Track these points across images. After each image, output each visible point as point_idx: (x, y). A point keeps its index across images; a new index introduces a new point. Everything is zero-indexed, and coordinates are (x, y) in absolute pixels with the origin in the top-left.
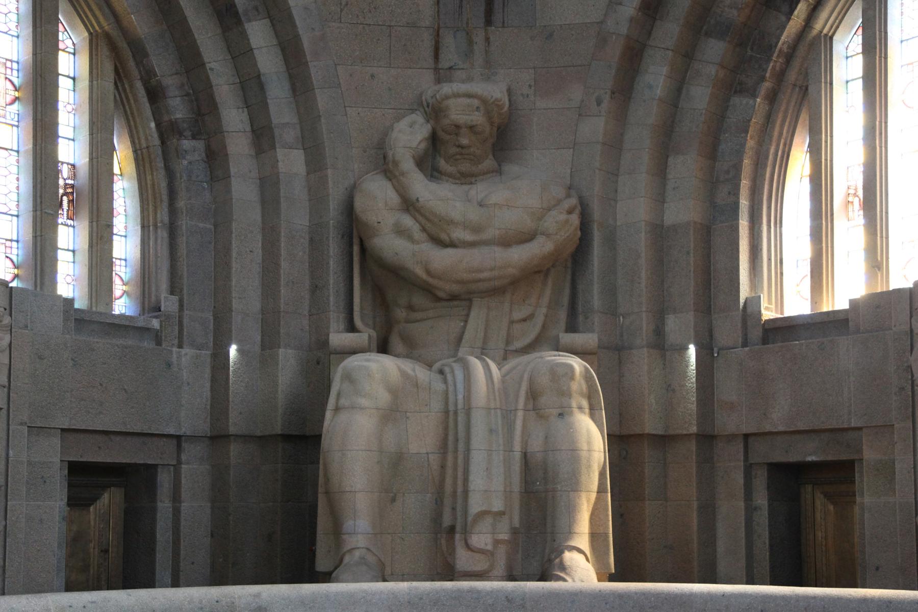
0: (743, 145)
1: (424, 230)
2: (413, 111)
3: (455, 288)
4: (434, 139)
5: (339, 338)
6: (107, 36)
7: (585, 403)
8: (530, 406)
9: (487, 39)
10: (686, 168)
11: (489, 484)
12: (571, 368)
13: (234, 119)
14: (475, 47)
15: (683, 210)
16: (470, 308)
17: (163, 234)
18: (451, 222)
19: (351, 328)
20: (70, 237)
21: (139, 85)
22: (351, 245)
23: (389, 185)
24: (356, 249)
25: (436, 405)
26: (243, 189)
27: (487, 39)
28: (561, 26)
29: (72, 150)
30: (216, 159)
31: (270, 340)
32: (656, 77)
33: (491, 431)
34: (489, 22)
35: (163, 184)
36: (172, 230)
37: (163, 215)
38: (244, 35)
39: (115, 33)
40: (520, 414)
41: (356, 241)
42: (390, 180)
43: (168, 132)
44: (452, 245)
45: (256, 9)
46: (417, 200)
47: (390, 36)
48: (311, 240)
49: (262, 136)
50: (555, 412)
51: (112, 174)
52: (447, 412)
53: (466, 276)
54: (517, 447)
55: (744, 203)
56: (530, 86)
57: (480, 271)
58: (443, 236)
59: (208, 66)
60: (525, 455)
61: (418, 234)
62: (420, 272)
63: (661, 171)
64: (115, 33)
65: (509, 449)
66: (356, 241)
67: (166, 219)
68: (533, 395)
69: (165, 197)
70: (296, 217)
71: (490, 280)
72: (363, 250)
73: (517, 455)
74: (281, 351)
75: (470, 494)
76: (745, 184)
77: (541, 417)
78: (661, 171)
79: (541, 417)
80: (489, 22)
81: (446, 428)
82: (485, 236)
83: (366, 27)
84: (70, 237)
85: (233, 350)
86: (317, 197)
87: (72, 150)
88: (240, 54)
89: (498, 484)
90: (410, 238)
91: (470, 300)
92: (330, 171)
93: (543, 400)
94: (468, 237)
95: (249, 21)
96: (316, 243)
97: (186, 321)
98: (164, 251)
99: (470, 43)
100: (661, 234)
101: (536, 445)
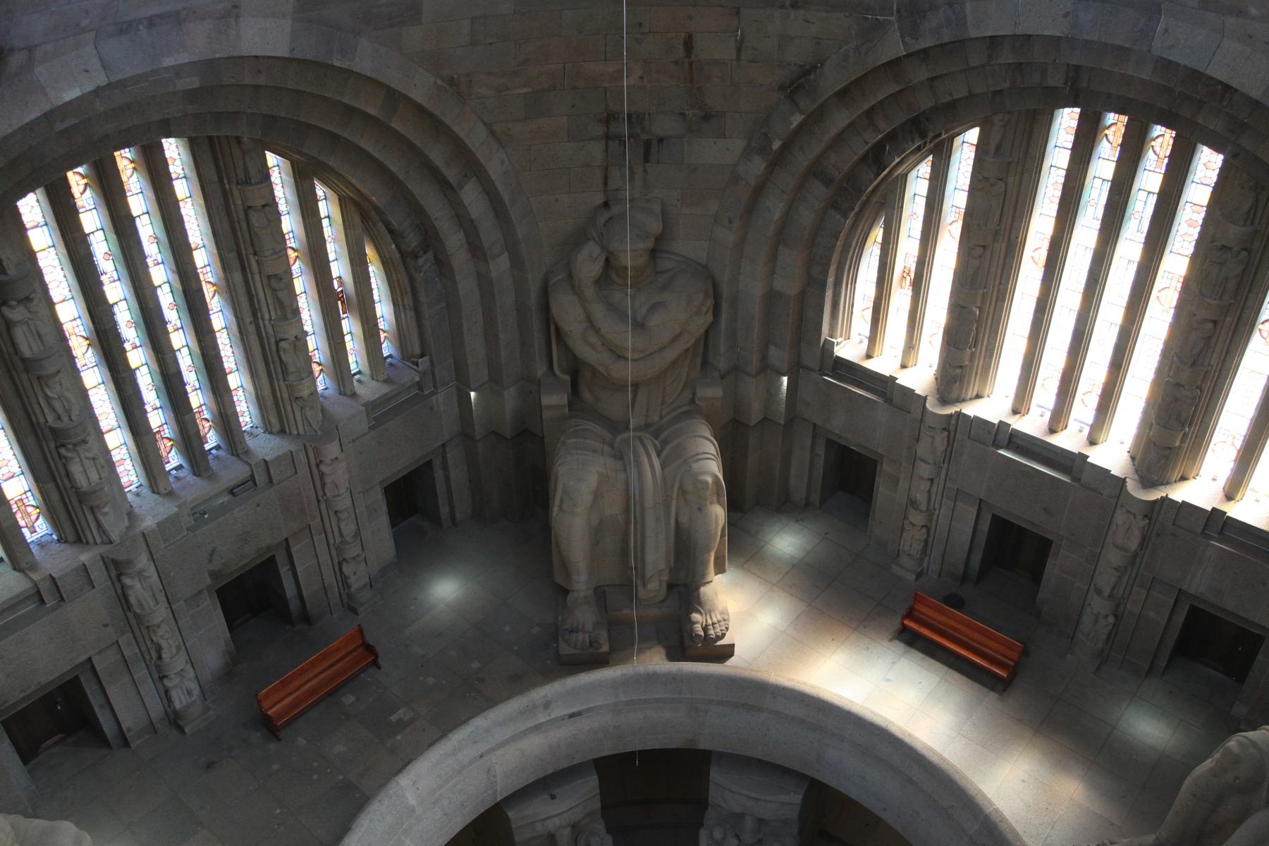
0: (834, 246)
9: (645, 171)
10: (792, 259)
12: (707, 483)
13: (454, 242)
15: (789, 285)
17: (411, 314)
20: (350, 325)
21: (380, 224)
27: (645, 171)
29: (339, 268)
30: (442, 264)
31: (494, 382)
32: (774, 207)
34: (646, 160)
35: (406, 281)
36: (417, 310)
37: (409, 301)
43: (407, 257)
45: (466, 176)
49: (476, 250)
51: (373, 302)
55: (831, 280)
63: (773, 257)
66: (552, 328)
67: (411, 304)
69: (409, 289)
72: (557, 329)
76: (829, 294)
78: (773, 257)
80: (646, 160)
84: (350, 325)
85: (473, 394)
87: (339, 268)
97: (437, 373)
98: (412, 323)
100: (771, 297)
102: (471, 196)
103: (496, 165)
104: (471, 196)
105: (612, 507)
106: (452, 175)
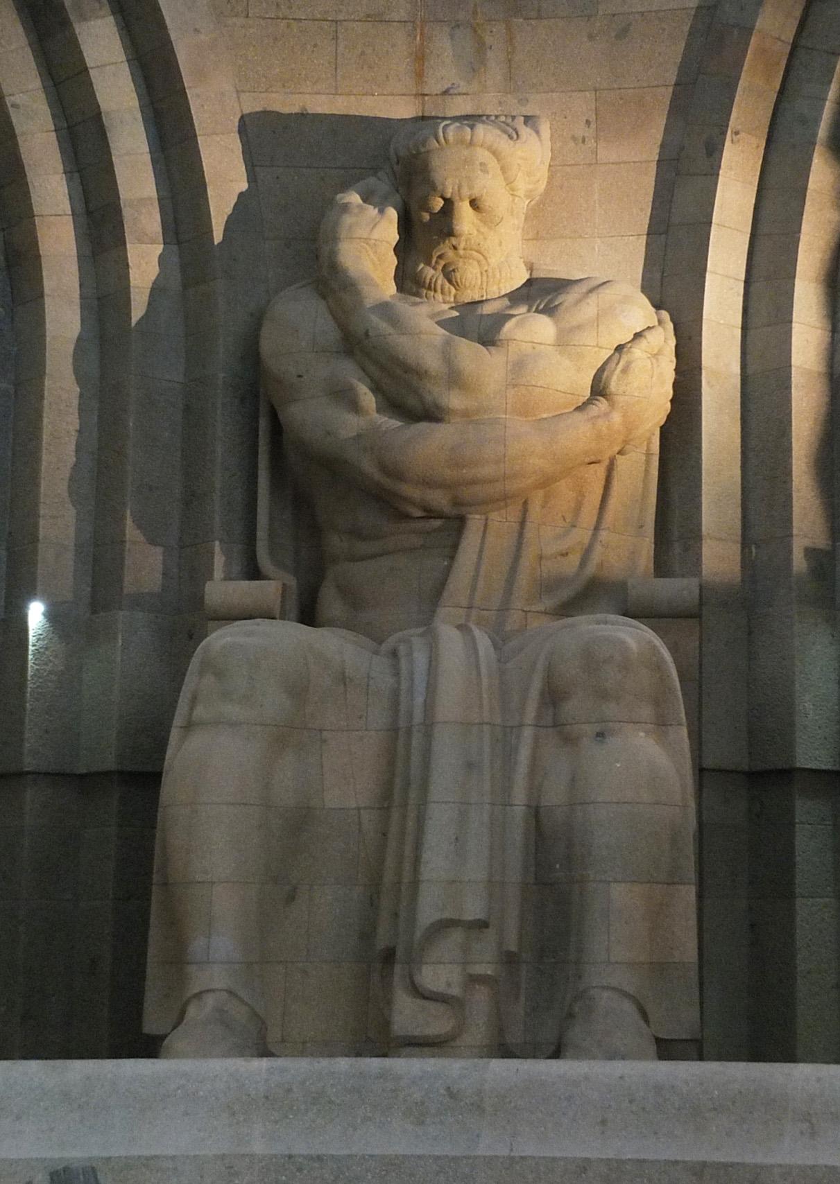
2: (375, 170)
5: (222, 588)
7: (646, 712)
11: (459, 866)
14: (489, 54)
19: (253, 572)
22: (255, 418)
23: (322, 306)
24: (263, 424)
28: (642, 14)
33: (470, 766)
38: (73, 46)
40: (528, 733)
41: (263, 409)
42: (324, 298)
46: (367, 334)
47: (336, 38)
48: (187, 409)
50: (590, 729)
52: (394, 730)
54: (520, 795)
56: (588, 122)
58: (412, 401)
60: (536, 813)
62: (368, 466)
66: (263, 409)
68: (553, 696)
72: (277, 429)
73: (519, 812)
75: (423, 887)
77: (569, 740)
79: (569, 740)
81: (391, 763)
83: (294, 24)
89: (476, 869)
93: (572, 707)
95: (83, 18)
99: (481, 48)
101: (555, 795)
102: (101, 45)
105: (344, 781)
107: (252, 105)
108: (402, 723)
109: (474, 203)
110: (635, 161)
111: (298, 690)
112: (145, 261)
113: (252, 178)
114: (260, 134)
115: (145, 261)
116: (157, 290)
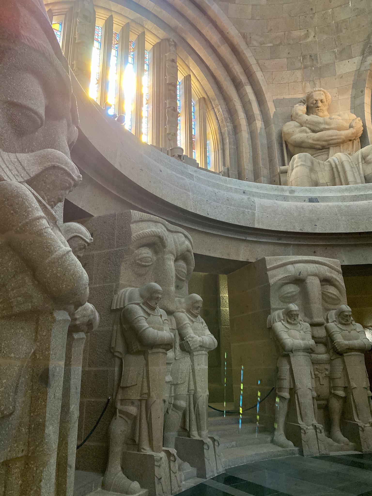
1: (310, 129)
3: (324, 143)
4: (307, 108)
6: (204, 98)
8: (364, 162)
16: (329, 151)
18: (320, 123)
24: (284, 145)
25: (327, 168)
26: (245, 135)
39: (206, 97)
44: (322, 130)
53: (327, 138)
54: (362, 172)
57: (332, 136)
58: (317, 129)
59: (234, 100)
60: (365, 177)
61: (308, 130)
62: (310, 141)
64: (206, 97)
65: (360, 174)
70: (262, 141)
71: (335, 139)
73: (363, 175)
74: (262, 178)
82: (333, 126)
86: (269, 135)
88: (242, 96)
90: (306, 132)
91: (329, 148)
92: (273, 125)
94: (327, 127)
95: (246, 85)
96: (270, 147)
99: (315, 84)
103: (259, 75)
104: (248, 89)
106: (243, 78)
107: (274, 98)
108: (334, 166)
109: (321, 101)
110: (346, 98)
111: (312, 163)
112: (259, 124)
113: (276, 110)
114: (277, 103)
115: (259, 124)
116: (261, 128)
